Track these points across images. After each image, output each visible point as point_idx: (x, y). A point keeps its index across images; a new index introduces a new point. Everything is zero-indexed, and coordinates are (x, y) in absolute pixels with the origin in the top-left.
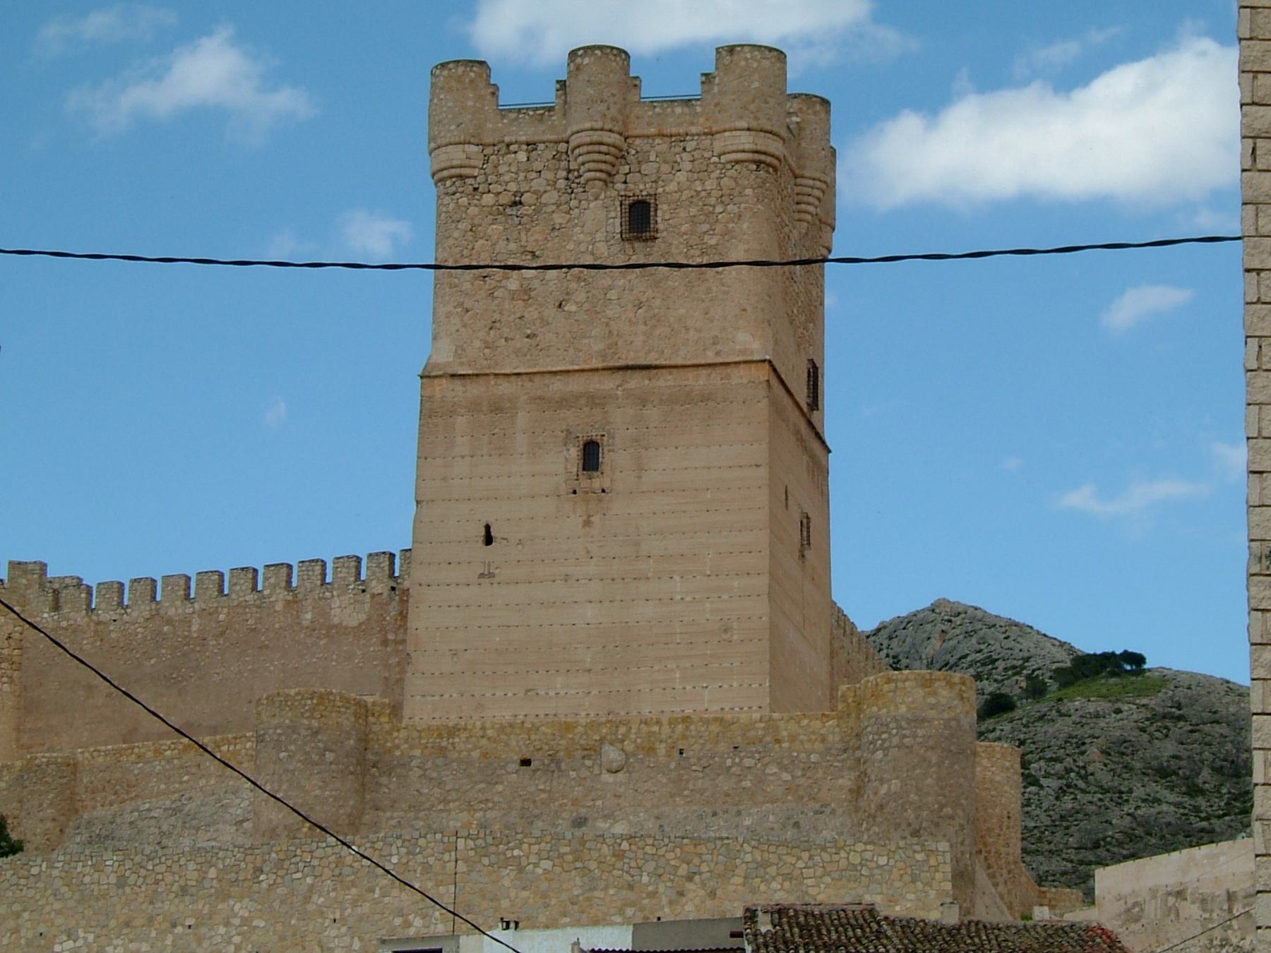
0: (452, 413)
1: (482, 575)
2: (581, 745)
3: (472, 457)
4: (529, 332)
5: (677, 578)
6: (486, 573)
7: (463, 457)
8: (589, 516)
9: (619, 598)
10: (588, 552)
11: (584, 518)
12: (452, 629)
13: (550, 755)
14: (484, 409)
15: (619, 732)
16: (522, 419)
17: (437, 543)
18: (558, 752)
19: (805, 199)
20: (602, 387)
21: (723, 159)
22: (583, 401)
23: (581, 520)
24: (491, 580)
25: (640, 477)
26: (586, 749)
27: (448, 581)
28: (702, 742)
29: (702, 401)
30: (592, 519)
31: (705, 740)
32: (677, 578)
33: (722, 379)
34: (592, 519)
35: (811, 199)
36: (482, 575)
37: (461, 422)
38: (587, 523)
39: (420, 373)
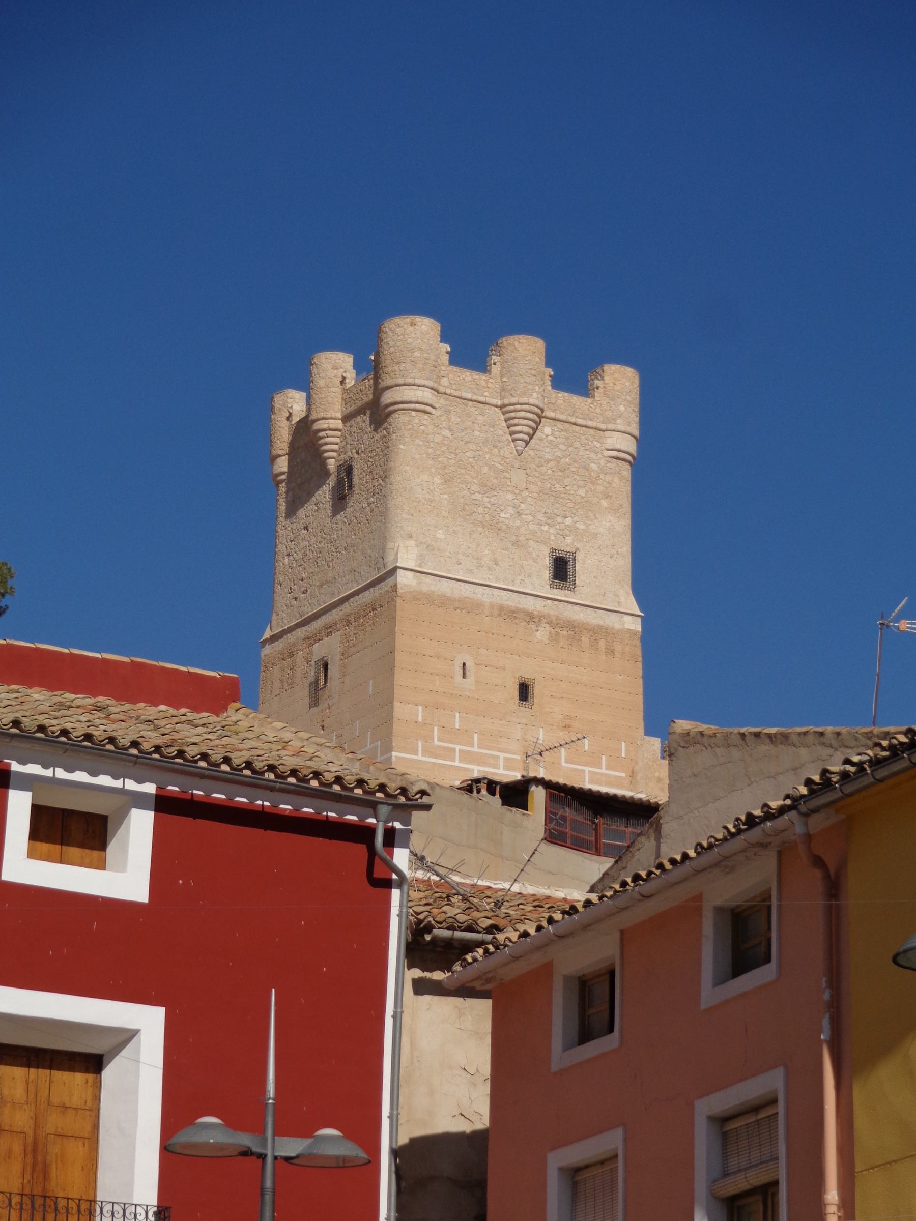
7: (276, 696)
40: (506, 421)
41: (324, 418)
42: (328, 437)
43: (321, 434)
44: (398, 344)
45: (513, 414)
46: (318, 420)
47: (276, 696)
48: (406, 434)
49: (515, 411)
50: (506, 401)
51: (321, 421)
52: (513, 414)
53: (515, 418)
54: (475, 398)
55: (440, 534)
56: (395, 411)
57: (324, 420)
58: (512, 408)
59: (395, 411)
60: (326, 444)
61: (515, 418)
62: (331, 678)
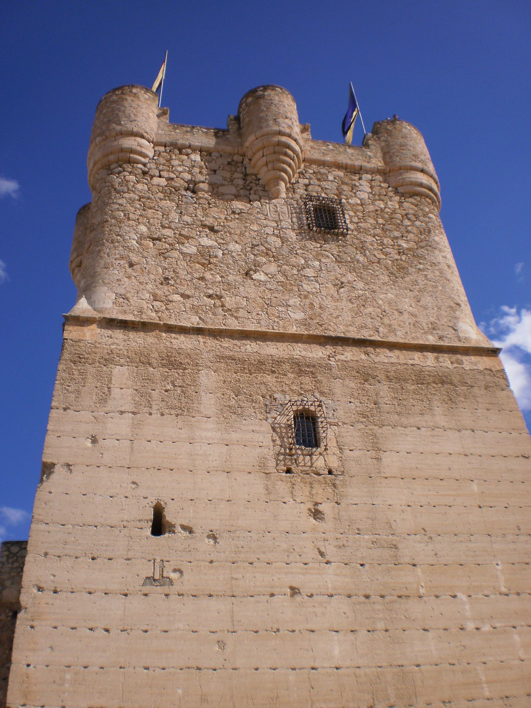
1: (150, 580)
3: (134, 413)
5: (462, 597)
6: (157, 577)
7: (122, 413)
9: (381, 625)
10: (322, 554)
12: (97, 669)
14: (153, 361)
17: (73, 526)
20: (310, 355)
23: (304, 508)
24: (166, 589)
25: (379, 459)
27: (91, 587)
32: (462, 597)
34: (320, 508)
36: (150, 580)
42: (293, 160)
43: (290, 152)
47: (122, 413)
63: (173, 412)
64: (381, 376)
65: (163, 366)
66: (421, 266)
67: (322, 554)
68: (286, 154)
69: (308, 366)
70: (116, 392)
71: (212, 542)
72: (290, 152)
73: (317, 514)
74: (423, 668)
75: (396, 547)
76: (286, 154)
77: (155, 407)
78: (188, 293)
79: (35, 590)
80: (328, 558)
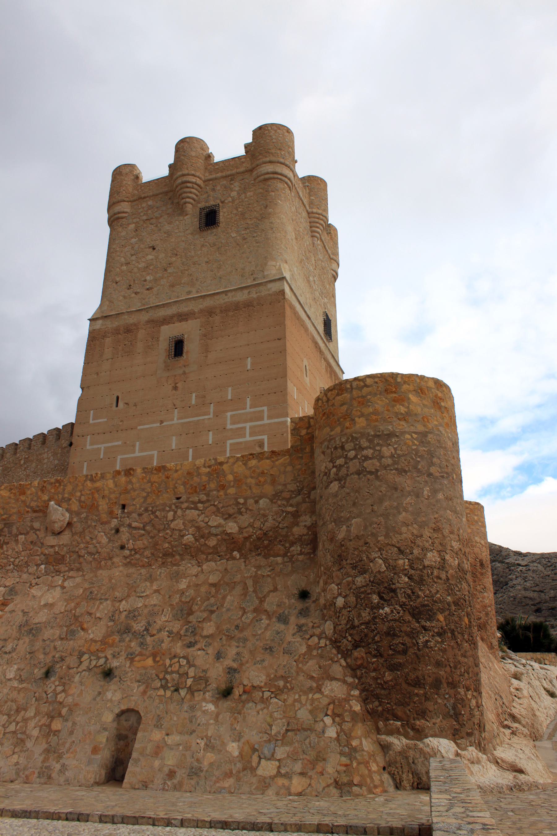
0: (104, 337)
2: (32, 508)
4: (148, 287)
7: (107, 360)
8: (176, 383)
9: (191, 431)
10: (175, 405)
11: (173, 385)
13: (4, 520)
14: (121, 332)
15: (66, 491)
16: (141, 334)
18: (10, 515)
19: (315, 224)
21: (257, 181)
22: (175, 319)
25: (206, 357)
26: (35, 511)
28: (145, 494)
29: (245, 308)
30: (177, 385)
31: (148, 493)
33: (256, 293)
34: (177, 385)
35: (318, 225)
37: (108, 340)
38: (175, 388)
39: (90, 317)
40: (310, 223)
41: (193, 175)
42: (193, 188)
43: (189, 185)
44: (280, 139)
45: (317, 220)
46: (188, 175)
47: (107, 360)
48: (283, 195)
49: (318, 218)
50: (315, 210)
51: (190, 177)
52: (317, 220)
53: (317, 223)
54: (303, 199)
55: (295, 269)
56: (274, 178)
57: (193, 177)
58: (317, 216)
59: (274, 178)
60: (191, 192)
61: (317, 223)
62: (187, 352)
63: (126, 354)
64: (218, 311)
65: (125, 333)
66: (255, 235)
67: (175, 405)
68: (187, 187)
69: (185, 316)
70: (106, 350)
71: (135, 407)
72: (189, 185)
73: (175, 388)
74: (205, 446)
75: (205, 397)
76: (187, 187)
77: (120, 354)
78: (138, 290)
79: (77, 437)
80: (176, 407)
